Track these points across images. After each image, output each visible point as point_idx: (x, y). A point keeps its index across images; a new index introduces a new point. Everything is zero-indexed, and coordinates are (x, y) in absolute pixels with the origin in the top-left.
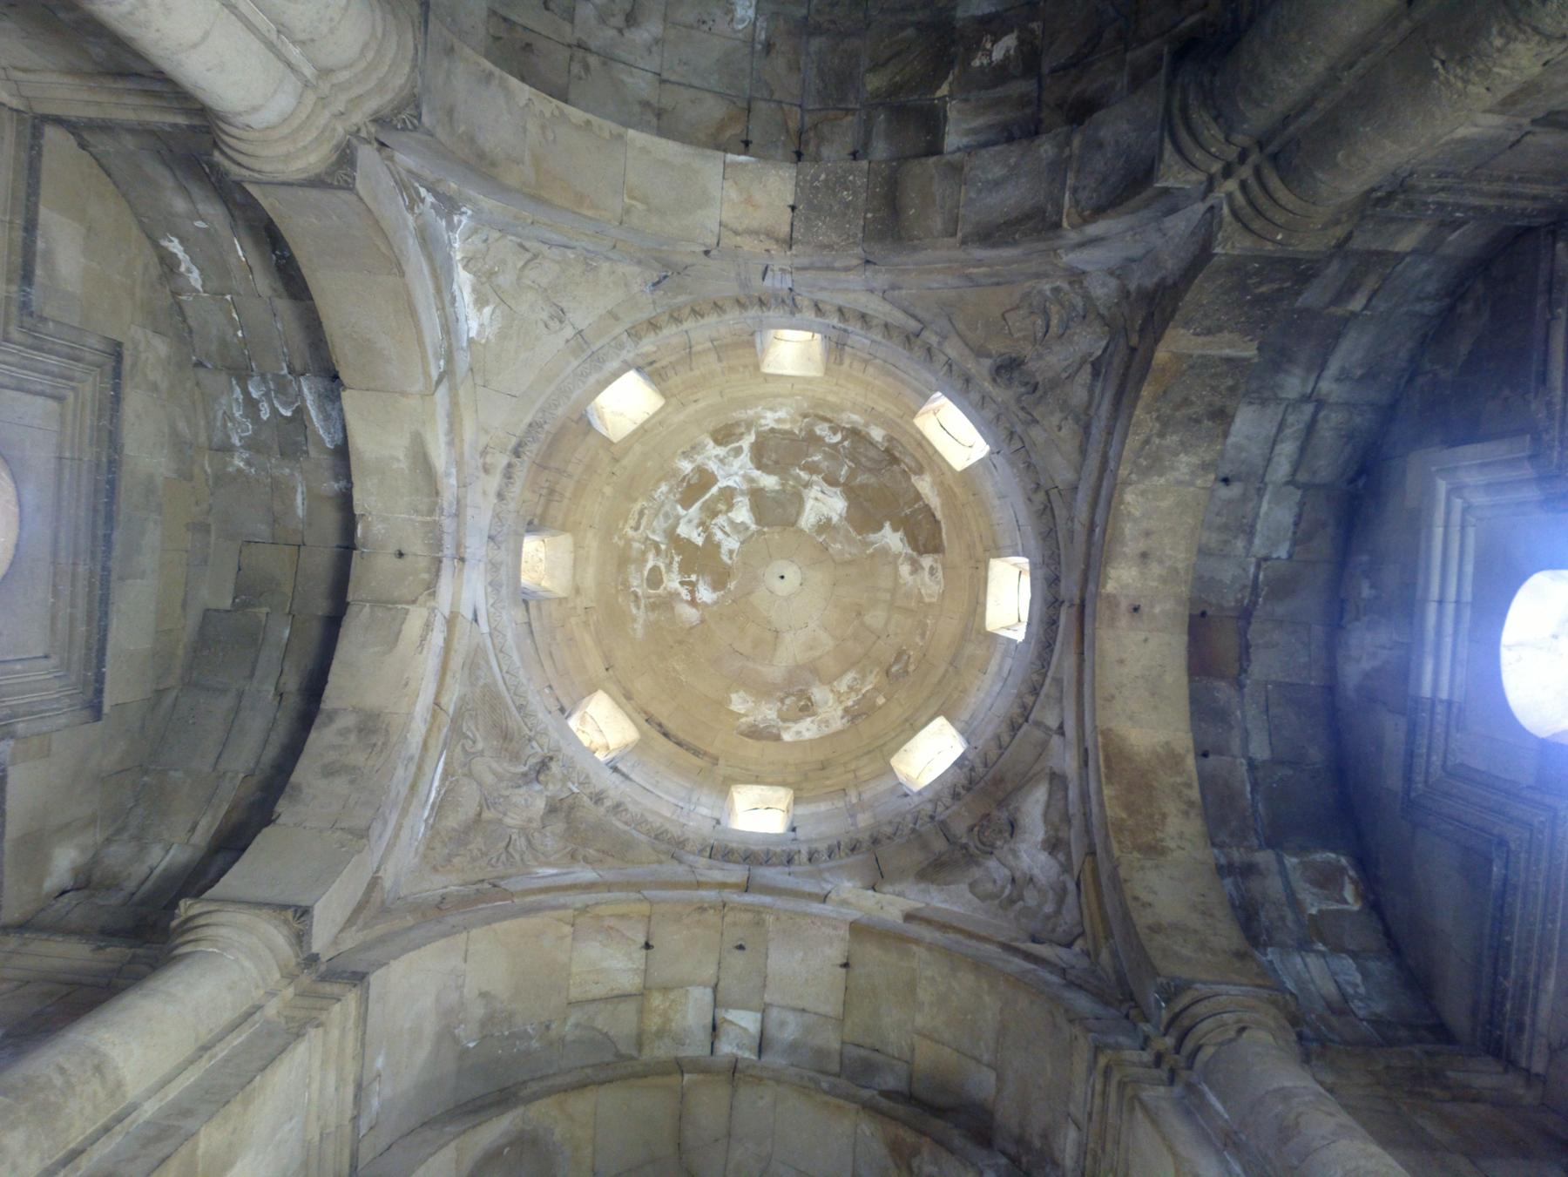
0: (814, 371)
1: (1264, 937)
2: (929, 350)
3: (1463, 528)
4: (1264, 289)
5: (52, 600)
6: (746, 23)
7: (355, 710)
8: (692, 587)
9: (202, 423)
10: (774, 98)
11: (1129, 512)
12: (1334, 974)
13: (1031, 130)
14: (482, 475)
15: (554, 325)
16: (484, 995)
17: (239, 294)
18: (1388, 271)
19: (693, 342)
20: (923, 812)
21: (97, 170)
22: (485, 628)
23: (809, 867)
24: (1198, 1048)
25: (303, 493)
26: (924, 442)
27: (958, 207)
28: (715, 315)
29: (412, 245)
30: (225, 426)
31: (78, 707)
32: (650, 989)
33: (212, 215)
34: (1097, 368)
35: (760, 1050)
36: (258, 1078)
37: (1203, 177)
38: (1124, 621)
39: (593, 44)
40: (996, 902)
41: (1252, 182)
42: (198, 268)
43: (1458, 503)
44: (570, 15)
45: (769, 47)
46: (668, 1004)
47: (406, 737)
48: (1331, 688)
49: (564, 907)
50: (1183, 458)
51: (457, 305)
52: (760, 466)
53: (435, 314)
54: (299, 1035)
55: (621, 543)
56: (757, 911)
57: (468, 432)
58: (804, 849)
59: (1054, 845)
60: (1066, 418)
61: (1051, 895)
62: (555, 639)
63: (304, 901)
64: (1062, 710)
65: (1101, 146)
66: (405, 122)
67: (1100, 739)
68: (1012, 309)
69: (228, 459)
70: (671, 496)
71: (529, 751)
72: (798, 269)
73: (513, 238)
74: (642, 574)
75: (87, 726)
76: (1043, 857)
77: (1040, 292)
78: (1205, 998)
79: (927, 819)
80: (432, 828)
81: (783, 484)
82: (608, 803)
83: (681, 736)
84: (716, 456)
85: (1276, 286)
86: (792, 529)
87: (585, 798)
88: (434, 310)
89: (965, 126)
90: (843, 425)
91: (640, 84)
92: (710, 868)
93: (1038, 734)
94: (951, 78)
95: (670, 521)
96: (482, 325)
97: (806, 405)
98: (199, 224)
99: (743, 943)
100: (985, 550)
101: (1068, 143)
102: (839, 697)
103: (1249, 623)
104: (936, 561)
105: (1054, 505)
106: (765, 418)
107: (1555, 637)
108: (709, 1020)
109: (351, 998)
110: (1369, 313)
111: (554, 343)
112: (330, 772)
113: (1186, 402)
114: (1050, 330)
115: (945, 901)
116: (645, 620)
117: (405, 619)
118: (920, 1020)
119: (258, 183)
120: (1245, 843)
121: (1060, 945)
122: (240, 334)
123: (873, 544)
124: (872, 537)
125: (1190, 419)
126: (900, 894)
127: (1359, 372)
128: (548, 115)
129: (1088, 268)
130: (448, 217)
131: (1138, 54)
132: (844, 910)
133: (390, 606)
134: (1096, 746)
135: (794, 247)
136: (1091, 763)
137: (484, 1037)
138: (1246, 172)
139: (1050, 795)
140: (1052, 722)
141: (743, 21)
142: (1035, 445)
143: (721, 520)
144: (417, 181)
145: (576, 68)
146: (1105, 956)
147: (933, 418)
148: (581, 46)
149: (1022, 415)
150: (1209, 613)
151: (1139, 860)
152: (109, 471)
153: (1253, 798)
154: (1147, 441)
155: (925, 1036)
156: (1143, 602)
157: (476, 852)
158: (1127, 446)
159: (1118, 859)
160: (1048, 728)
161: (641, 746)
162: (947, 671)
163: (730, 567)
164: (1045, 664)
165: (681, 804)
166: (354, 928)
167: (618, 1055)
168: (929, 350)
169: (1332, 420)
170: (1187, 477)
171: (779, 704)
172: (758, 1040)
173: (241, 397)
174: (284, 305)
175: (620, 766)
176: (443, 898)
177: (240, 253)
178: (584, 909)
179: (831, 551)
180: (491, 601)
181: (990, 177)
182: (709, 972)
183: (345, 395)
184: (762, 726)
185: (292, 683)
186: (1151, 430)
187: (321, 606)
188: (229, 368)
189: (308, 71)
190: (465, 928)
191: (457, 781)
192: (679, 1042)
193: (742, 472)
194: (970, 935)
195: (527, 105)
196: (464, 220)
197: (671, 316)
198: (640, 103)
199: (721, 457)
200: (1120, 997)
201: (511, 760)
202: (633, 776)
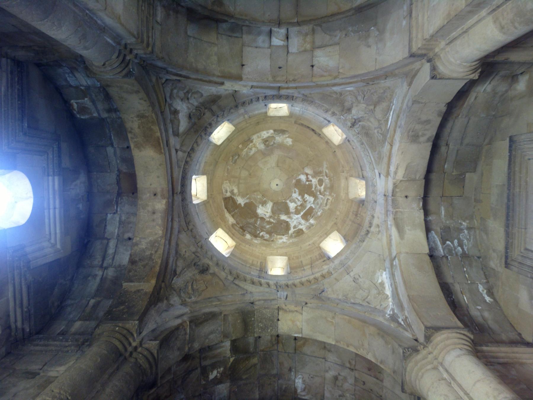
0: (270, 258)
1: (101, 90)
2: (231, 273)
3: (50, 234)
4: (122, 307)
5: (527, 179)
6: (298, 378)
7: (420, 143)
8: (308, 180)
9: (478, 237)
10: (287, 354)
11: (160, 227)
12: (77, 79)
13: (202, 350)
14: (380, 224)
15: (357, 277)
16: (369, 46)
17: (465, 283)
18: (83, 314)
19: (310, 269)
20: (221, 118)
21: (515, 326)
22: (376, 171)
23: (259, 96)
24: (117, 57)
25: (442, 215)
26: (232, 236)
27: (224, 324)
28: (303, 281)
29: (406, 304)
30: (470, 237)
31: (518, 141)
32: (311, 51)
33: (475, 311)
34: (175, 273)
35: (271, 31)
36: (445, 23)
37: (144, 346)
38: (159, 190)
39: (347, 371)
40: (193, 91)
41: (127, 346)
42: (480, 292)
43: (53, 241)
44: (356, 379)
45: (290, 370)
46: (304, 45)
47: (401, 135)
48: (89, 172)
49: (342, 78)
50: (144, 247)
51: (390, 283)
52: (287, 222)
53: (397, 280)
54: (432, 36)
55: (333, 194)
56: (275, 81)
57: (385, 240)
58: (261, 101)
59: (175, 112)
60: (184, 255)
61: (175, 96)
62: (353, 164)
63: (433, 81)
64: (177, 158)
65: (179, 349)
66: (408, 351)
67: (163, 151)
68: (204, 290)
69: (468, 225)
70: (316, 211)
71: (359, 129)
72: (276, 299)
73: (372, 306)
74: (325, 183)
75: (514, 134)
76: (179, 108)
77: (195, 297)
78: (117, 73)
79: (219, 116)
80: (391, 102)
81: (279, 217)
82: (330, 112)
83: (308, 130)
84: (302, 225)
85: (118, 309)
86: (275, 202)
87: (338, 114)
88: (397, 283)
89: (224, 349)
90: (260, 239)
91: (332, 357)
92: (293, 93)
93: (184, 149)
94: (230, 364)
95: (316, 202)
96: (382, 276)
97: (273, 245)
98: (479, 308)
99: (279, 69)
100: (209, 202)
101: (189, 349)
102: (255, 146)
103: (118, 192)
104: (226, 195)
105: (186, 225)
106: (286, 239)
107: (16, 202)
108: (290, 40)
109: (414, 49)
110: (88, 299)
111: (356, 270)
112: (428, 122)
113: (144, 266)
114: (191, 283)
115: (211, 89)
116: (323, 168)
117: (404, 175)
118: (216, 49)
119: (458, 328)
120: (111, 119)
121: (170, 80)
122: (465, 269)
123: (247, 199)
124: (247, 201)
125: (143, 260)
126: (227, 90)
127: (90, 278)
128: (361, 349)
129: (180, 306)
130: (394, 313)
131: (169, 377)
132: (245, 84)
133: (409, 179)
134: (164, 149)
135: (277, 307)
136: (165, 142)
137: (368, 31)
138: (130, 349)
139: (178, 129)
140: (180, 153)
141: (299, 378)
142: (193, 245)
143: (299, 203)
144: (404, 327)
145: (353, 363)
146: (154, 79)
147: (229, 245)
148: (352, 370)
149: (198, 255)
150: (131, 194)
151: (146, 113)
152: (508, 224)
153: (110, 134)
154: (156, 252)
155: (213, 43)
156: (153, 197)
157: (375, 94)
158: (163, 249)
159: (153, 113)
160: (181, 151)
161: (321, 127)
162: (219, 159)
163: (295, 187)
164: (184, 171)
165: (305, 111)
166: (416, 69)
167: (321, 26)
168: (231, 273)
169: (97, 261)
170: (142, 240)
171: (275, 142)
172: (272, 35)
173: (464, 247)
174: (450, 280)
175: (327, 122)
176: (386, 79)
177: (465, 298)
178: (335, 78)
179: (261, 195)
180: (375, 180)
181: (214, 335)
182: (290, 58)
183: (427, 251)
184: (281, 134)
185: (443, 149)
186: (155, 256)
187: (434, 176)
188: (468, 257)
189: (441, 369)
190: (377, 70)
191: (383, 119)
192: (299, 32)
193: (293, 220)
194: (201, 80)
195: (368, 353)
196: (388, 312)
197: (317, 280)
198: (331, 352)
199: (300, 225)
200: (147, 67)
201: (365, 126)
202: (323, 119)
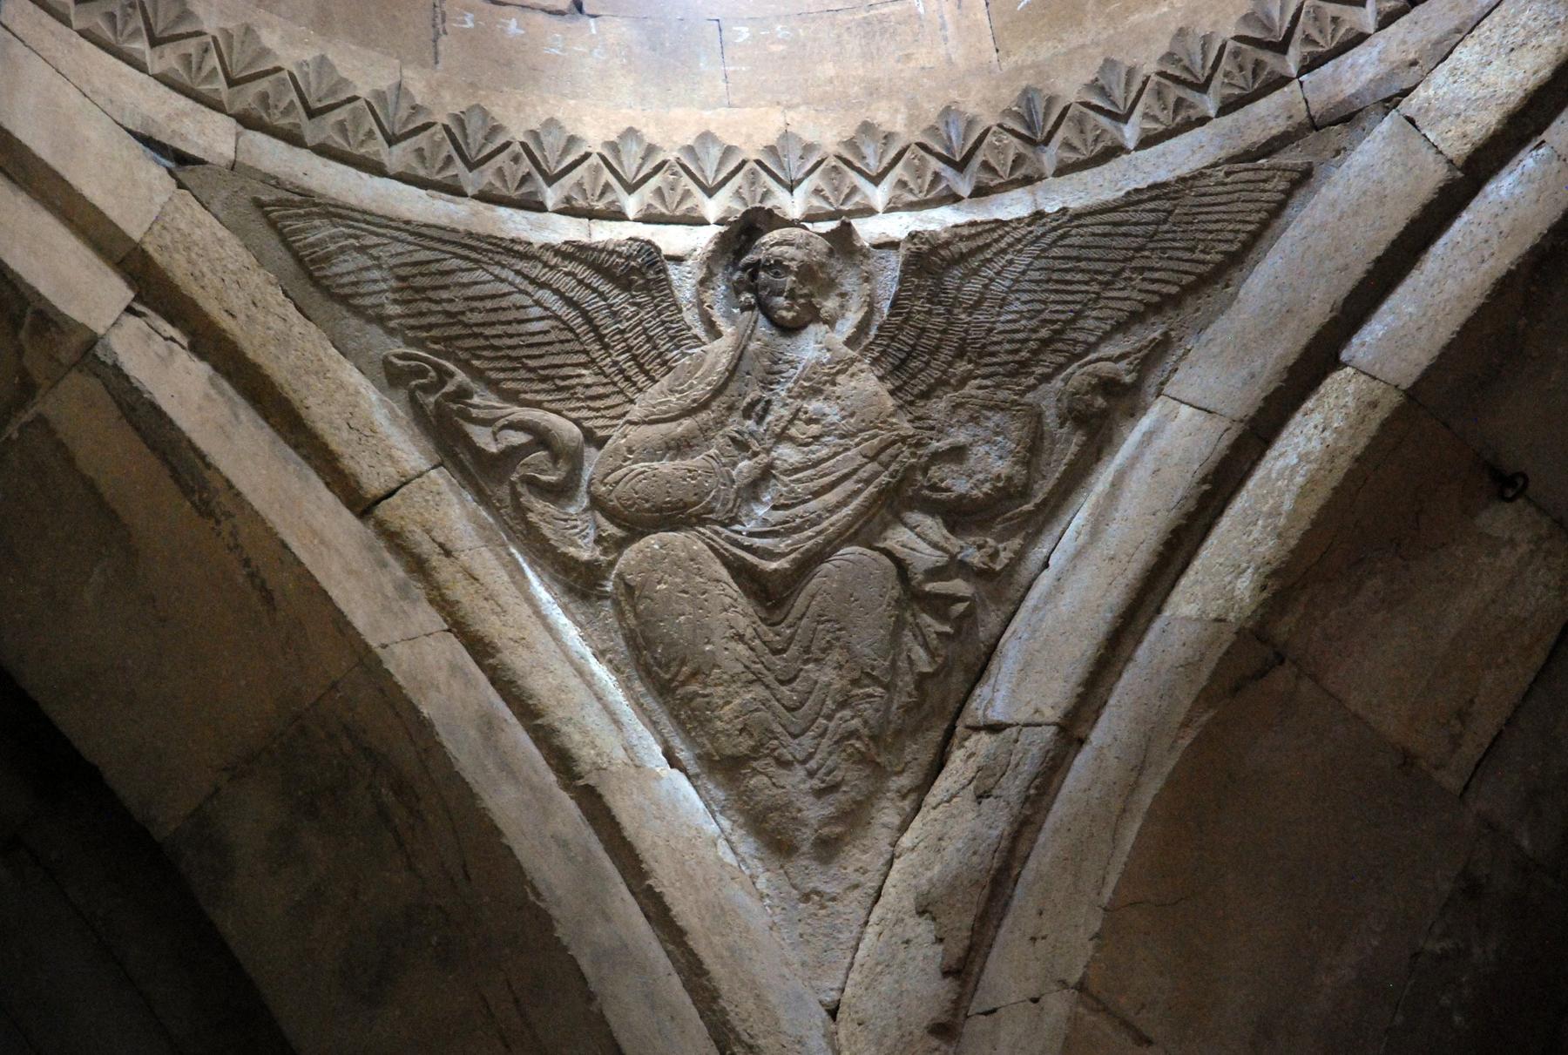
117: (60, 445)
